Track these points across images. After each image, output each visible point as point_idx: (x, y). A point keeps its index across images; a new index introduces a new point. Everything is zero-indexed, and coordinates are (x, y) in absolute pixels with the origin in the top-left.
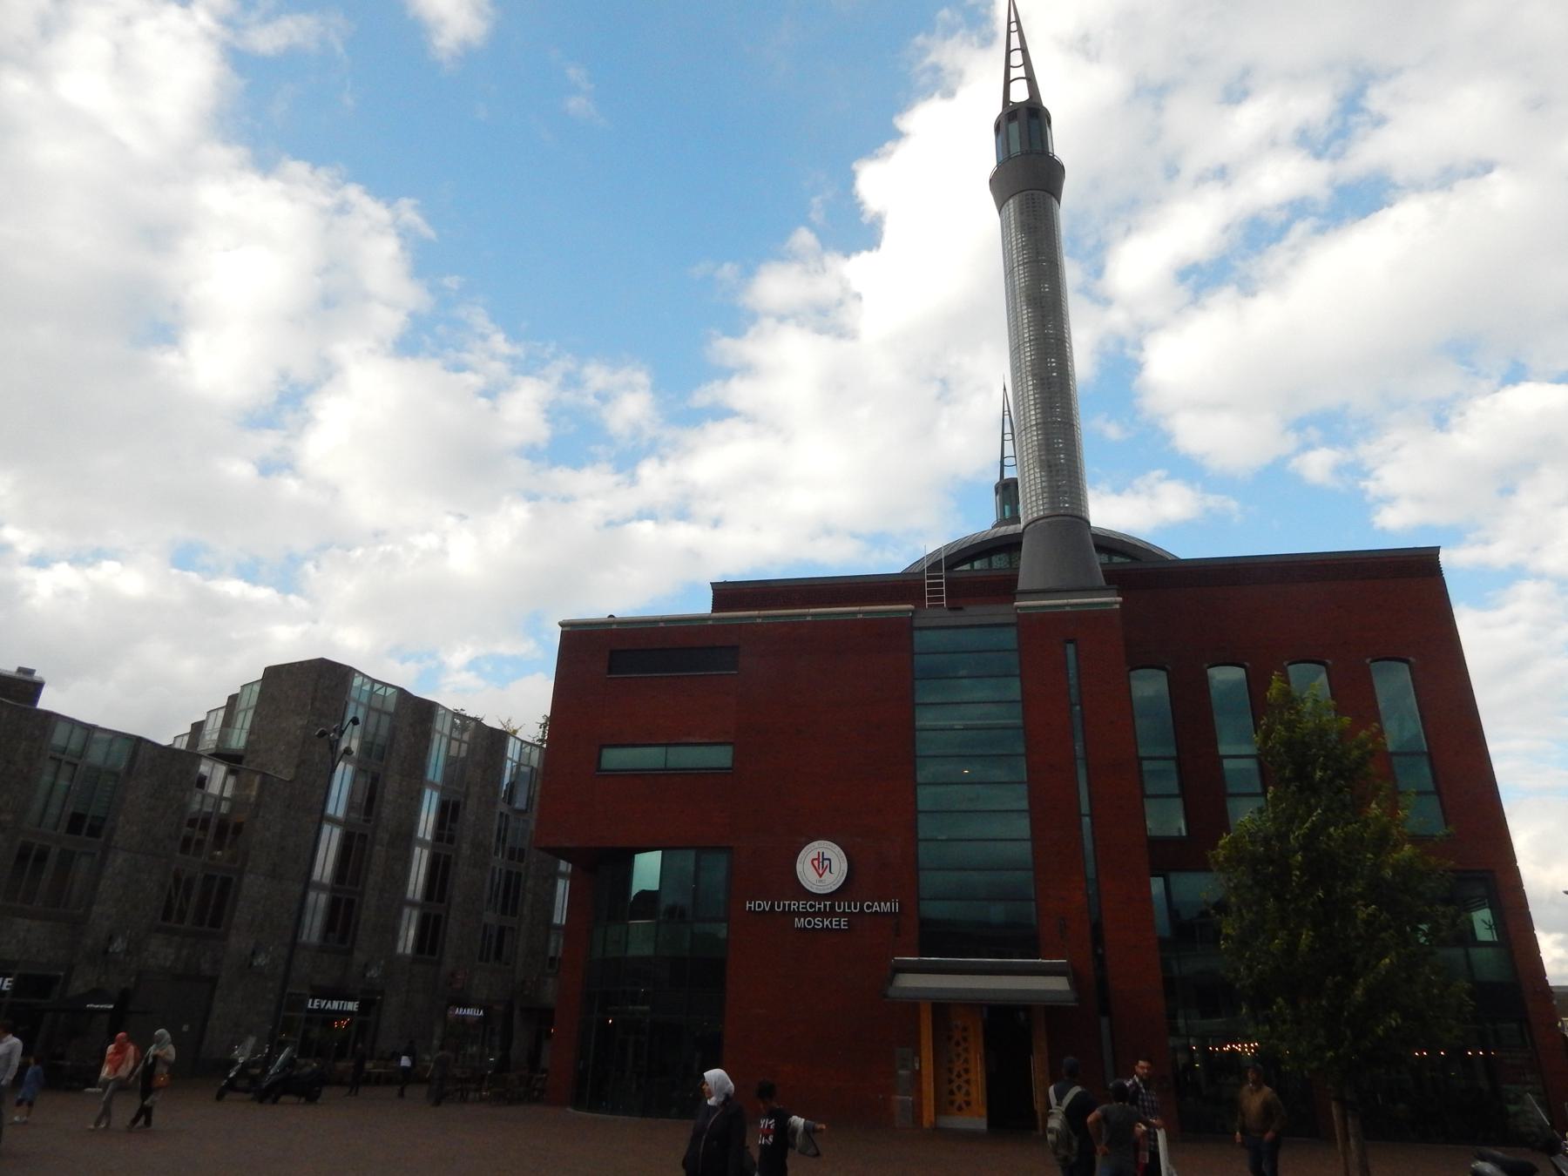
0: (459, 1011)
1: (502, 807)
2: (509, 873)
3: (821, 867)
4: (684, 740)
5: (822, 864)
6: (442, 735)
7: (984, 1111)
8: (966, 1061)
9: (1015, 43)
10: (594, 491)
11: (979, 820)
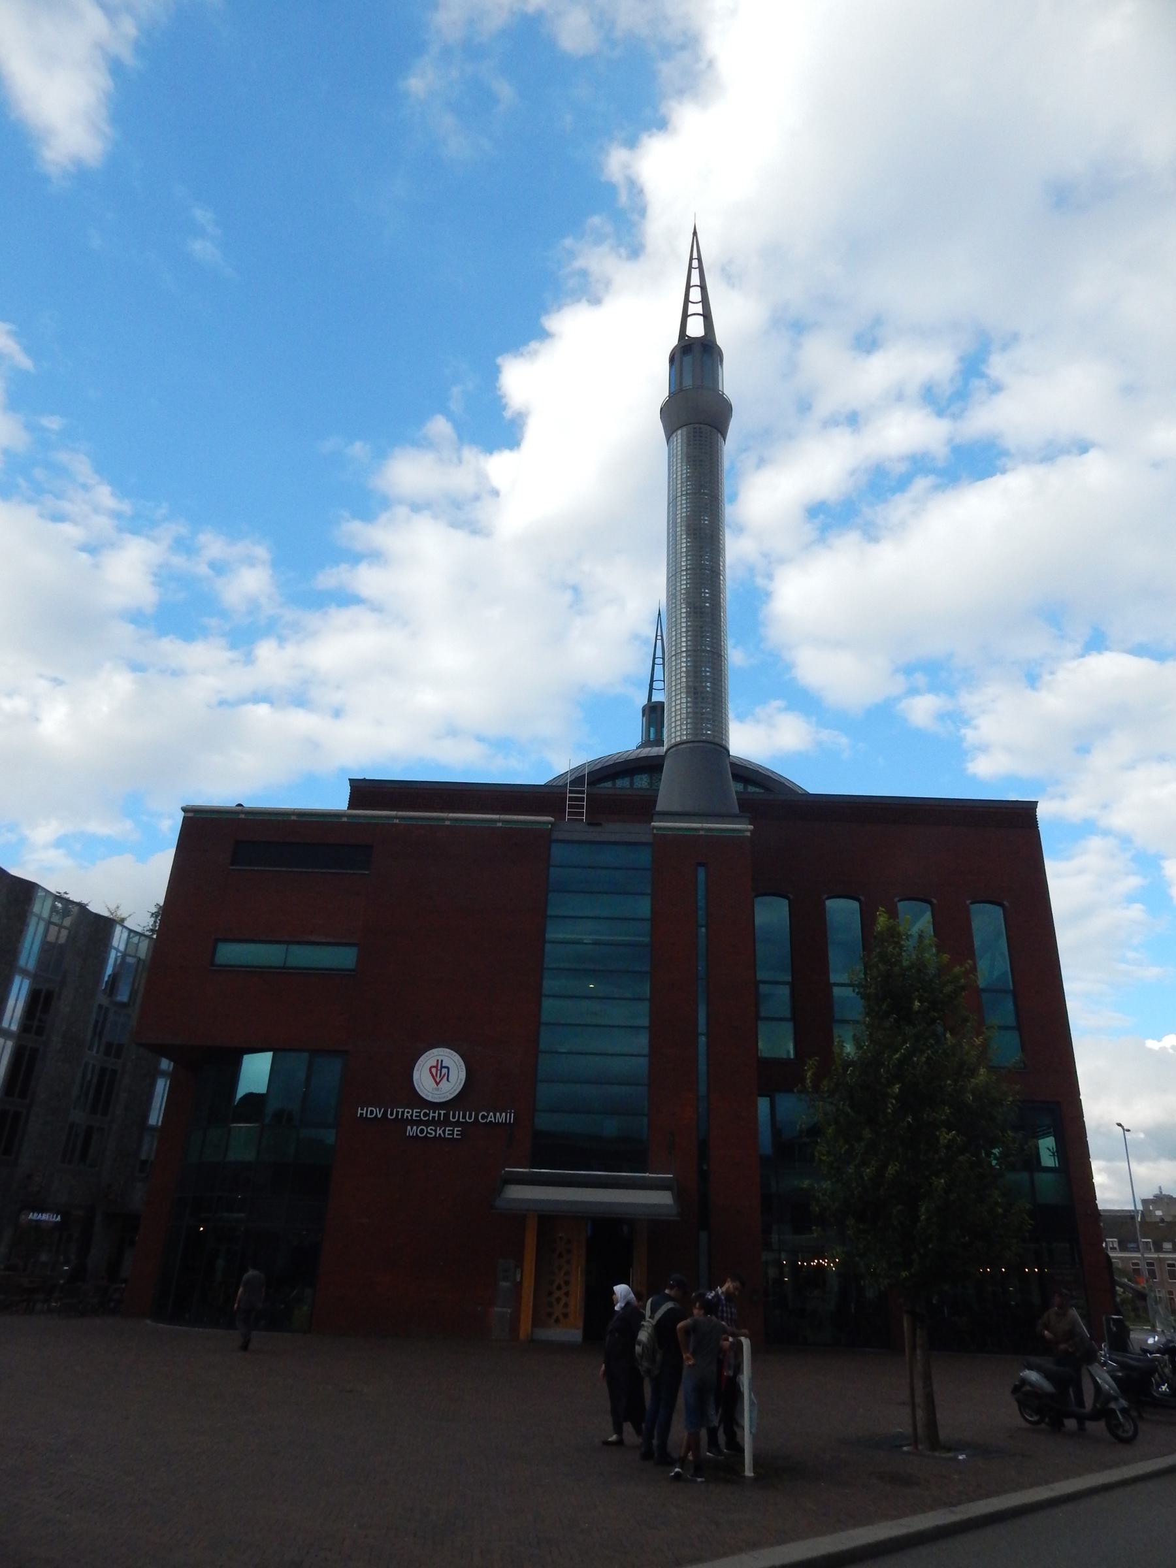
0: (33, 1216)
1: (103, 1000)
2: (103, 1070)
3: (439, 1074)
4: (313, 938)
5: (440, 1072)
6: (40, 918)
8: (567, 1273)
9: (695, 280)
10: (207, 669)
11: (600, 1037)
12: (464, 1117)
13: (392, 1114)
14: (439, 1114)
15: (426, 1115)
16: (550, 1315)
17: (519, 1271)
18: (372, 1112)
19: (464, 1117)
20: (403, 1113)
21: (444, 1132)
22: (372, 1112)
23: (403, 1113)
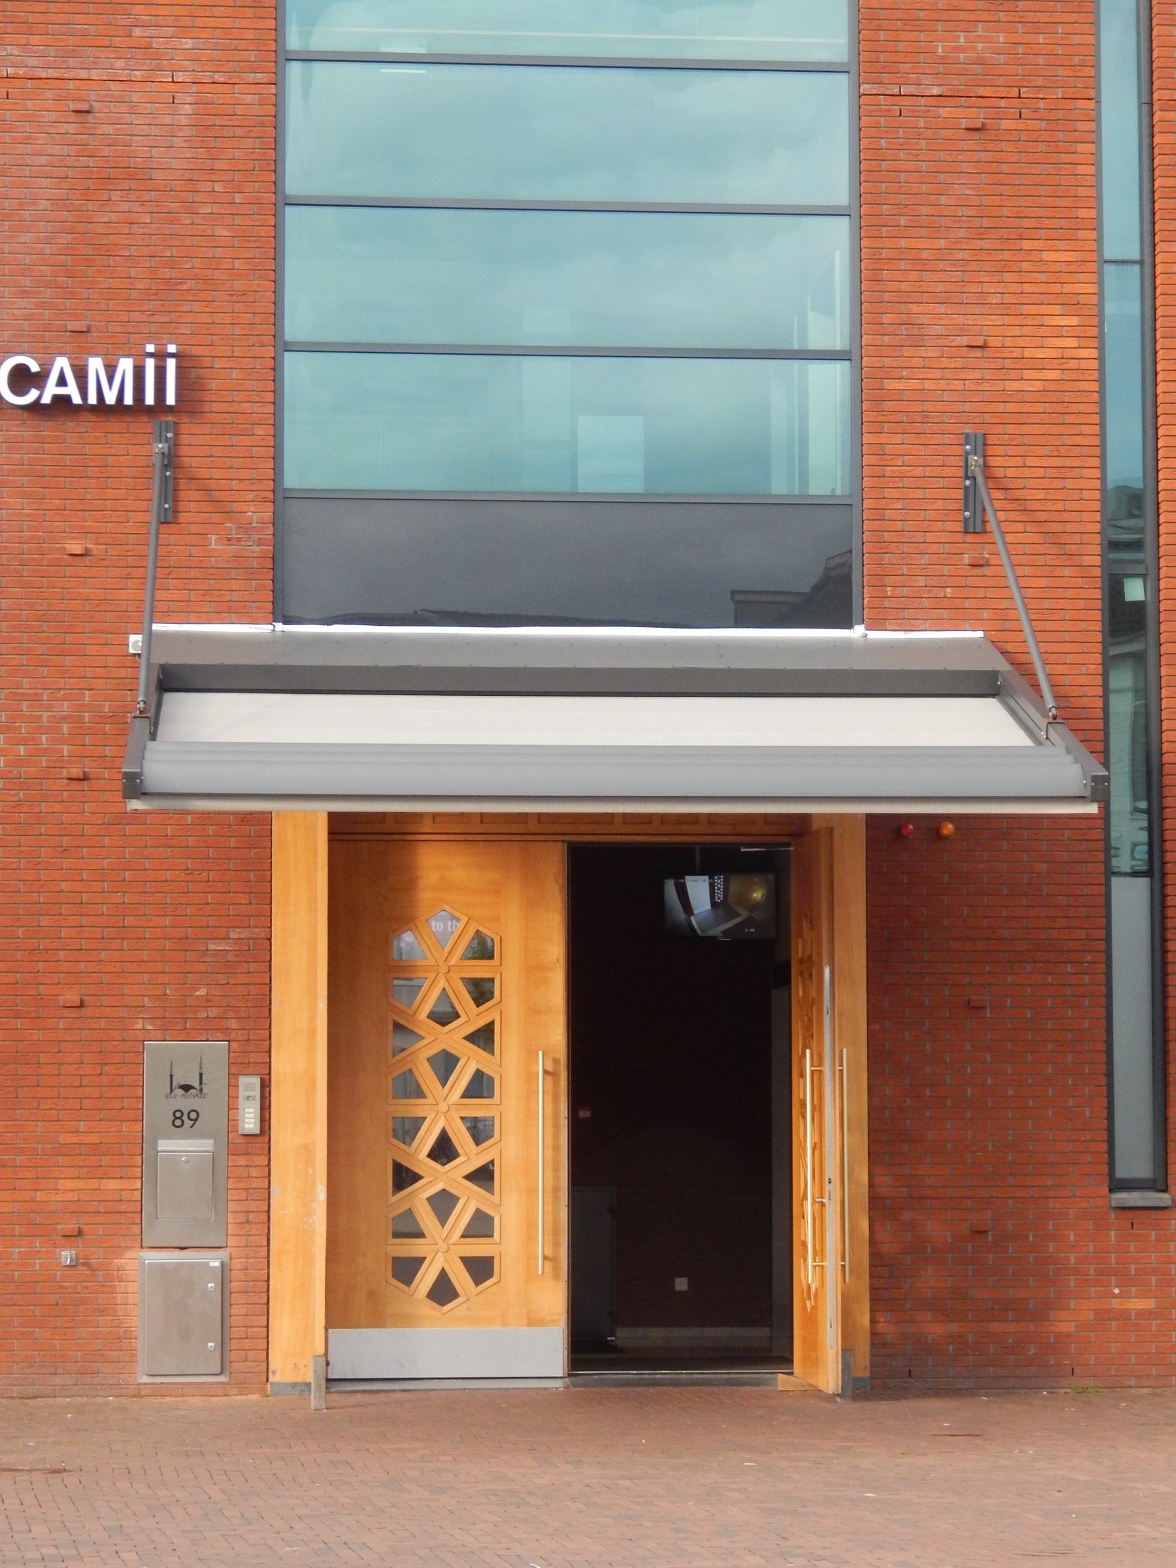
7: (554, 1299)
8: (480, 1086)
16: (406, 1269)
17: (249, 1085)
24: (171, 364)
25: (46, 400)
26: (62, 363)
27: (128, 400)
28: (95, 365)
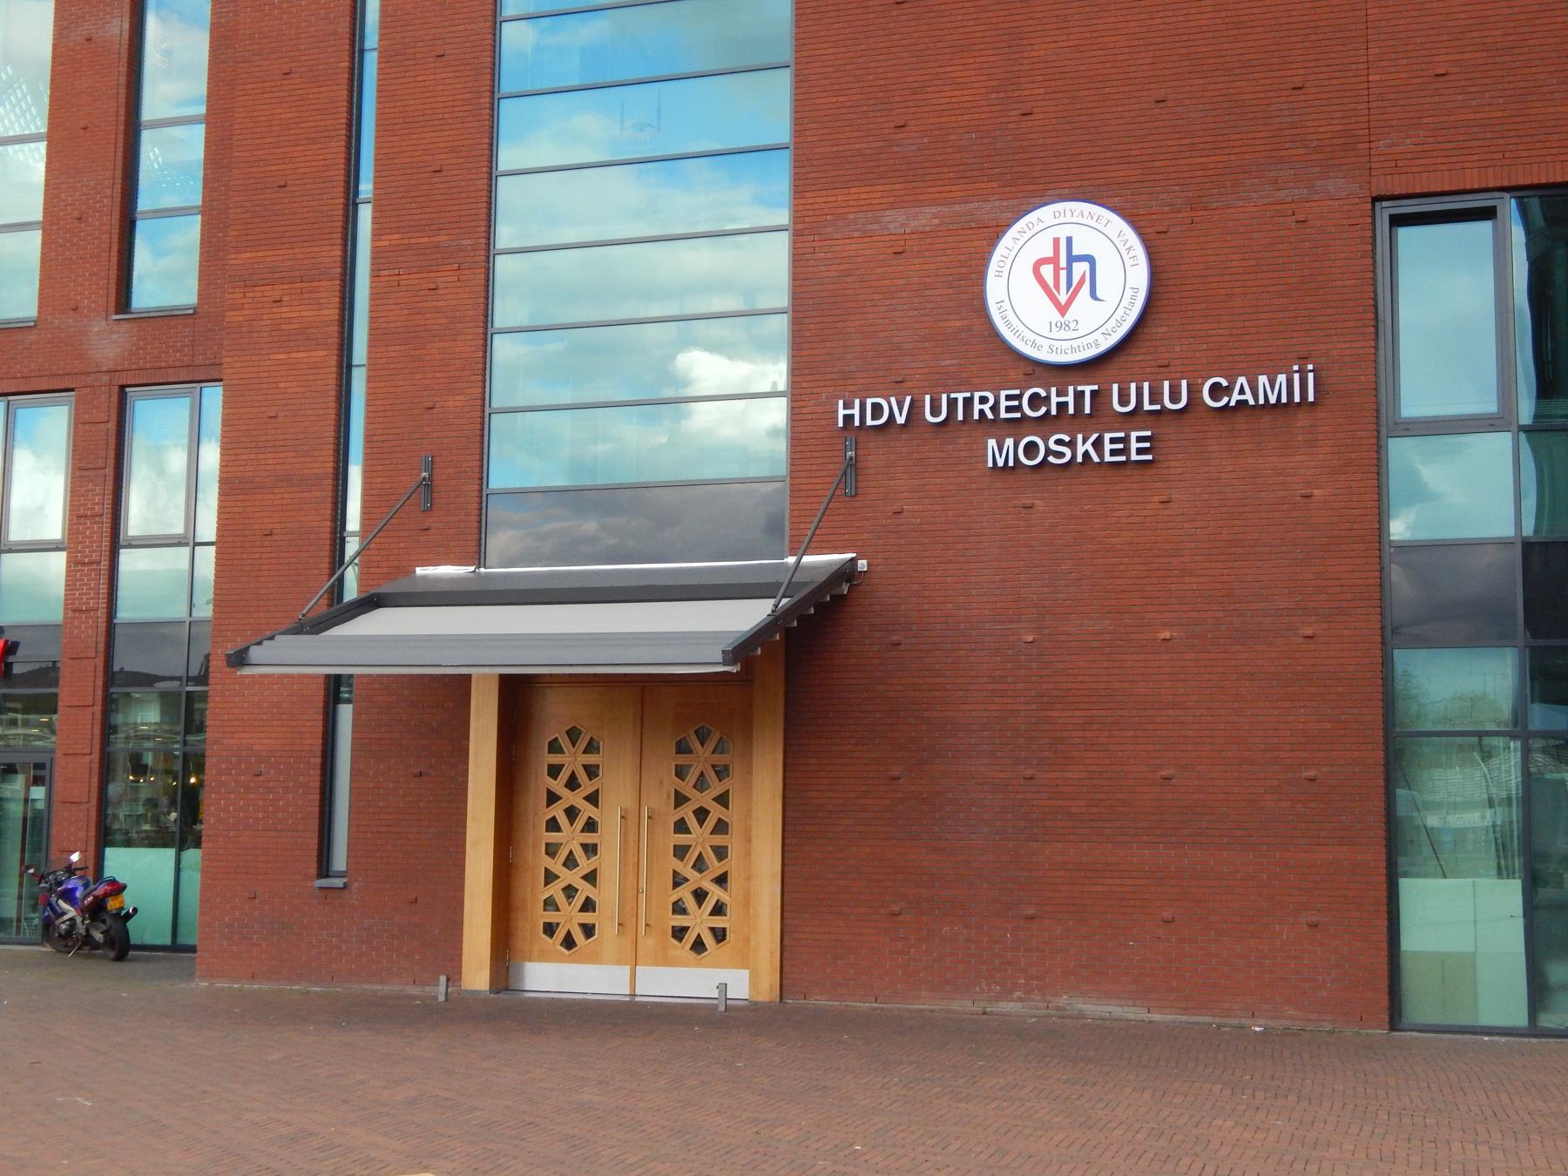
5: (1066, 273)
12: (1155, 397)
13: (935, 411)
14: (1079, 396)
15: (1035, 401)
18: (877, 409)
19: (1155, 397)
20: (968, 402)
21: (1098, 445)
22: (877, 409)
23: (968, 402)
24: (1311, 375)
25: (1233, 403)
26: (1242, 380)
27: (1284, 400)
28: (1263, 380)
